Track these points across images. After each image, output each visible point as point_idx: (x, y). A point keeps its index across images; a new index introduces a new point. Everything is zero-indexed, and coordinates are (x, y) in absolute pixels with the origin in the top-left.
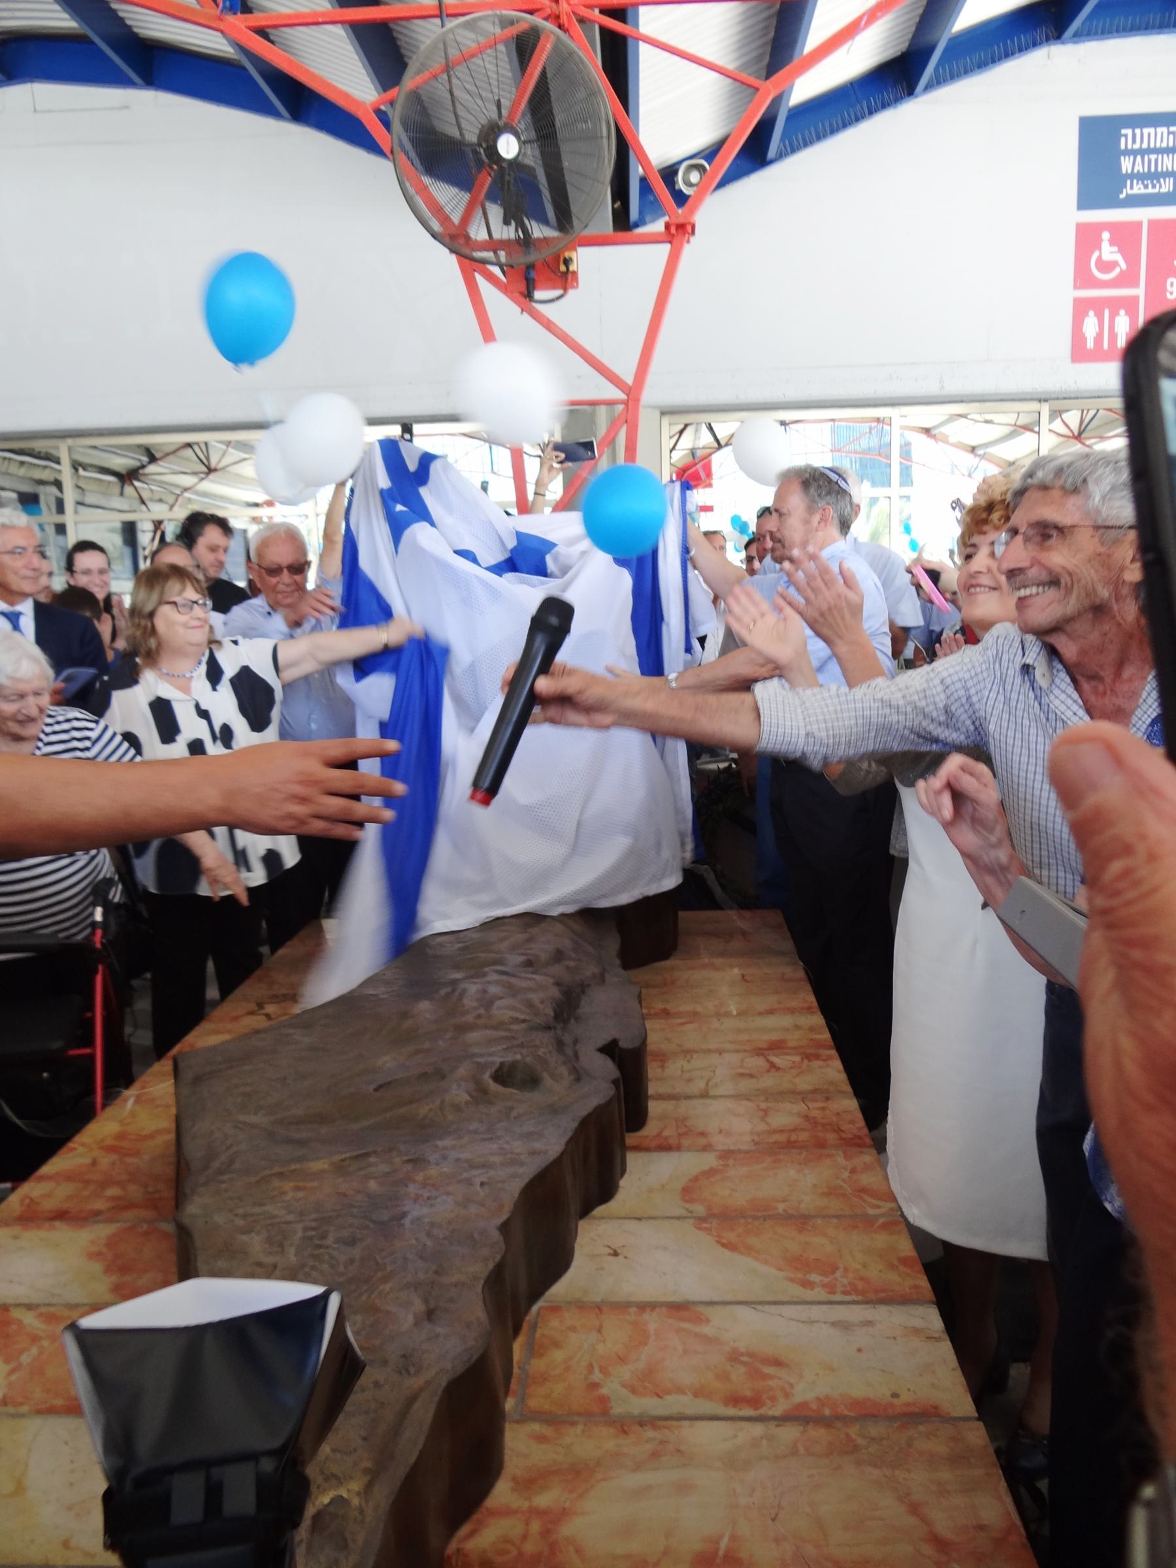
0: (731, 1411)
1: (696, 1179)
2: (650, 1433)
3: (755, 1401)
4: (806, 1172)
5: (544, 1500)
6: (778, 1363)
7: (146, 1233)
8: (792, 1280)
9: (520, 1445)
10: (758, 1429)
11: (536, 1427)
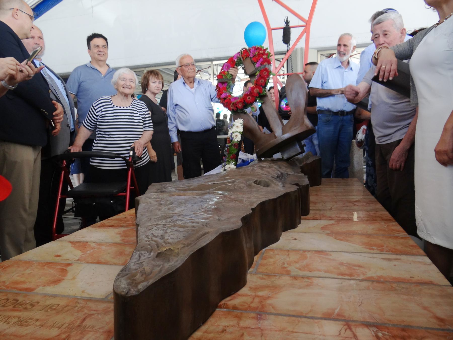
0: (340, 277)
1: (327, 225)
2: (307, 280)
3: (351, 275)
5: (260, 294)
8: (366, 248)
9: (252, 278)
10: (352, 282)
11: (261, 276)
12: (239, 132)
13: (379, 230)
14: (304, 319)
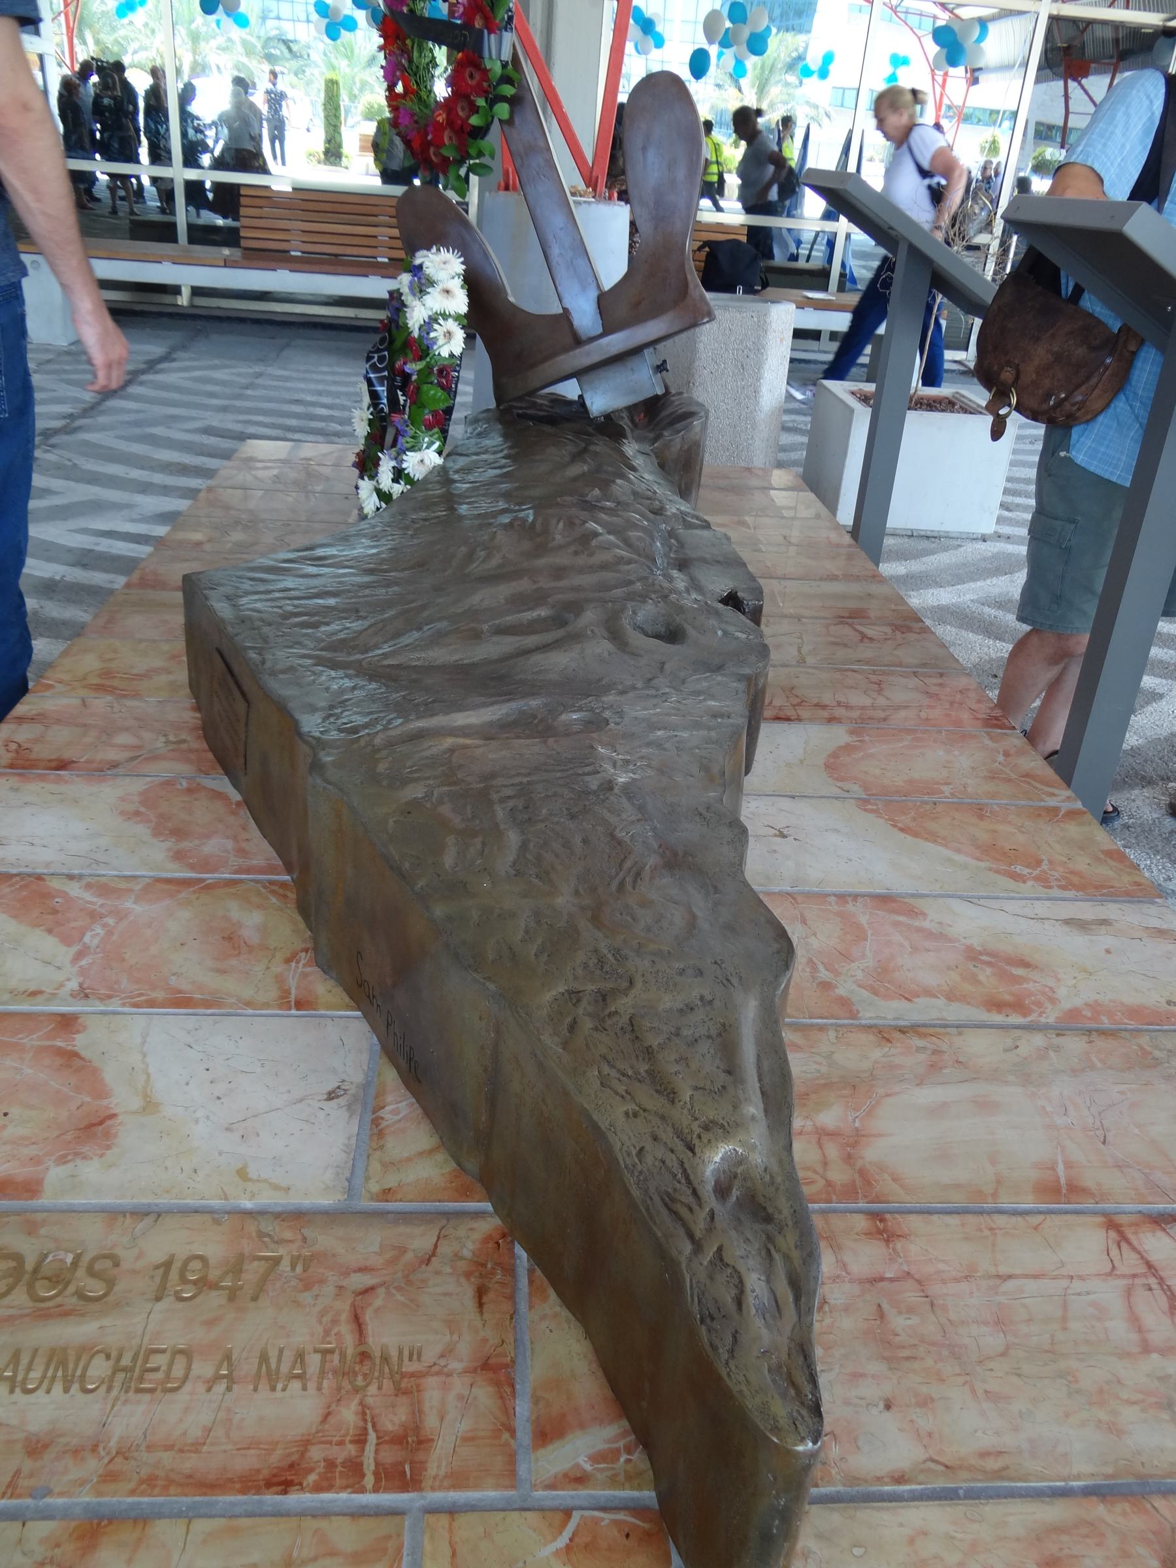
1: (834, 755)
4: (956, 753)
6: (1026, 965)
7: (189, 791)
8: (997, 872)
10: (1038, 1040)
12: (457, 318)
13: (993, 776)
14: (1001, 1220)
